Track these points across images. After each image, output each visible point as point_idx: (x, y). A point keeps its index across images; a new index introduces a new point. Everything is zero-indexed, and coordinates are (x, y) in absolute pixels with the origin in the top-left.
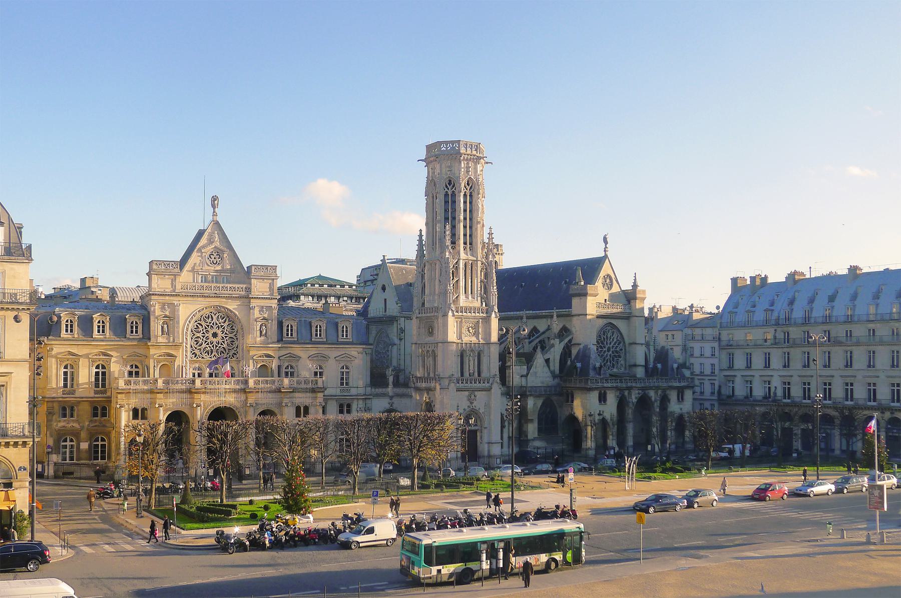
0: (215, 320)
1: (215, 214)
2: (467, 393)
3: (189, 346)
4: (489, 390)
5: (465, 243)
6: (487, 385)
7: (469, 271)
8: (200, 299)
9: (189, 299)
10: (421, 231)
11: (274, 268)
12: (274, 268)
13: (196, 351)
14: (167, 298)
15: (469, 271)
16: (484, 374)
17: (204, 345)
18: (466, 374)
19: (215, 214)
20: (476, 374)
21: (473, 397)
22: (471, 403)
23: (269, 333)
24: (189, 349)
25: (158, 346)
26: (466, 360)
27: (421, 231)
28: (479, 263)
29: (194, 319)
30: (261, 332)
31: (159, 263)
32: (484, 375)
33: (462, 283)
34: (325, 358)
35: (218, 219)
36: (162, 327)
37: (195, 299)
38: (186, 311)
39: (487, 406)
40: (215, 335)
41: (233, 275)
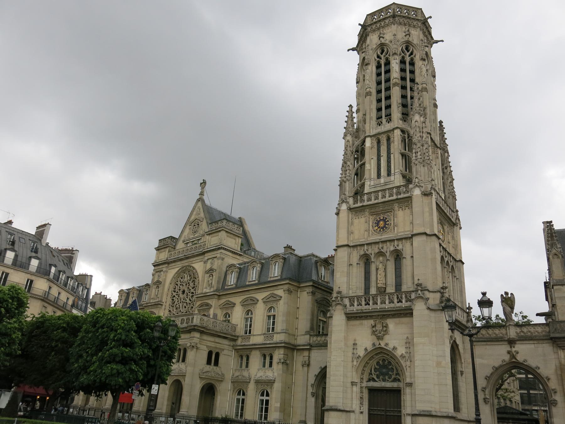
0: (186, 279)
1: (202, 194)
2: (372, 322)
3: (168, 304)
4: (408, 313)
5: (379, 118)
6: (404, 304)
7: (384, 148)
9: (173, 264)
14: (161, 267)
15: (384, 148)
16: (407, 286)
18: (373, 291)
19: (202, 194)
20: (391, 289)
21: (379, 327)
22: (379, 338)
24: (167, 308)
26: (373, 268)
28: (398, 133)
32: (404, 288)
33: (370, 166)
34: (255, 301)
39: (409, 343)
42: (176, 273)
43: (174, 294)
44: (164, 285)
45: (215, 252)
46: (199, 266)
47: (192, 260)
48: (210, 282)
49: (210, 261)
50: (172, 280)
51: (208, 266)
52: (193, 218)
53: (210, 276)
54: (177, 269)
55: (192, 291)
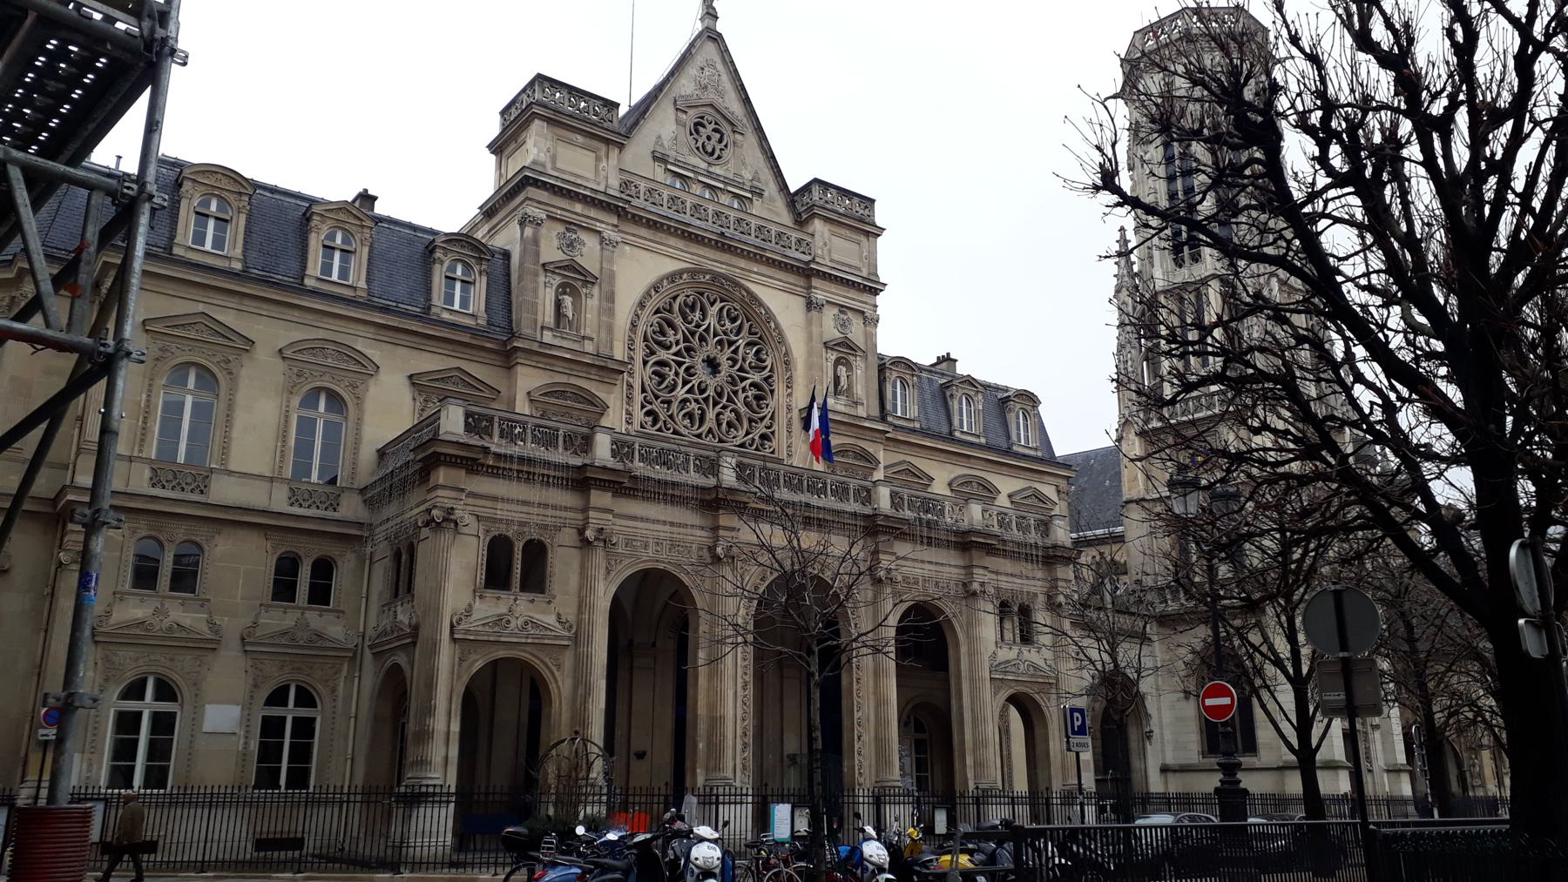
0: (711, 320)
8: (672, 241)
9: (643, 232)
10: (1122, 229)
11: (873, 201)
12: (873, 201)
13: (657, 406)
14: (578, 208)
17: (681, 392)
23: (859, 390)
24: (638, 397)
25: (543, 357)
27: (1122, 229)
29: (655, 302)
30: (837, 380)
31: (555, 84)
35: (720, 27)
36: (558, 305)
37: (660, 237)
38: (638, 270)
40: (713, 365)
41: (757, 202)
42: (672, 277)
43: (663, 355)
44: (610, 298)
45: (853, 294)
46: (781, 303)
47: (742, 263)
48: (843, 381)
49: (830, 313)
50: (648, 295)
51: (828, 325)
52: (686, 86)
53: (837, 362)
54: (672, 266)
55: (756, 377)
